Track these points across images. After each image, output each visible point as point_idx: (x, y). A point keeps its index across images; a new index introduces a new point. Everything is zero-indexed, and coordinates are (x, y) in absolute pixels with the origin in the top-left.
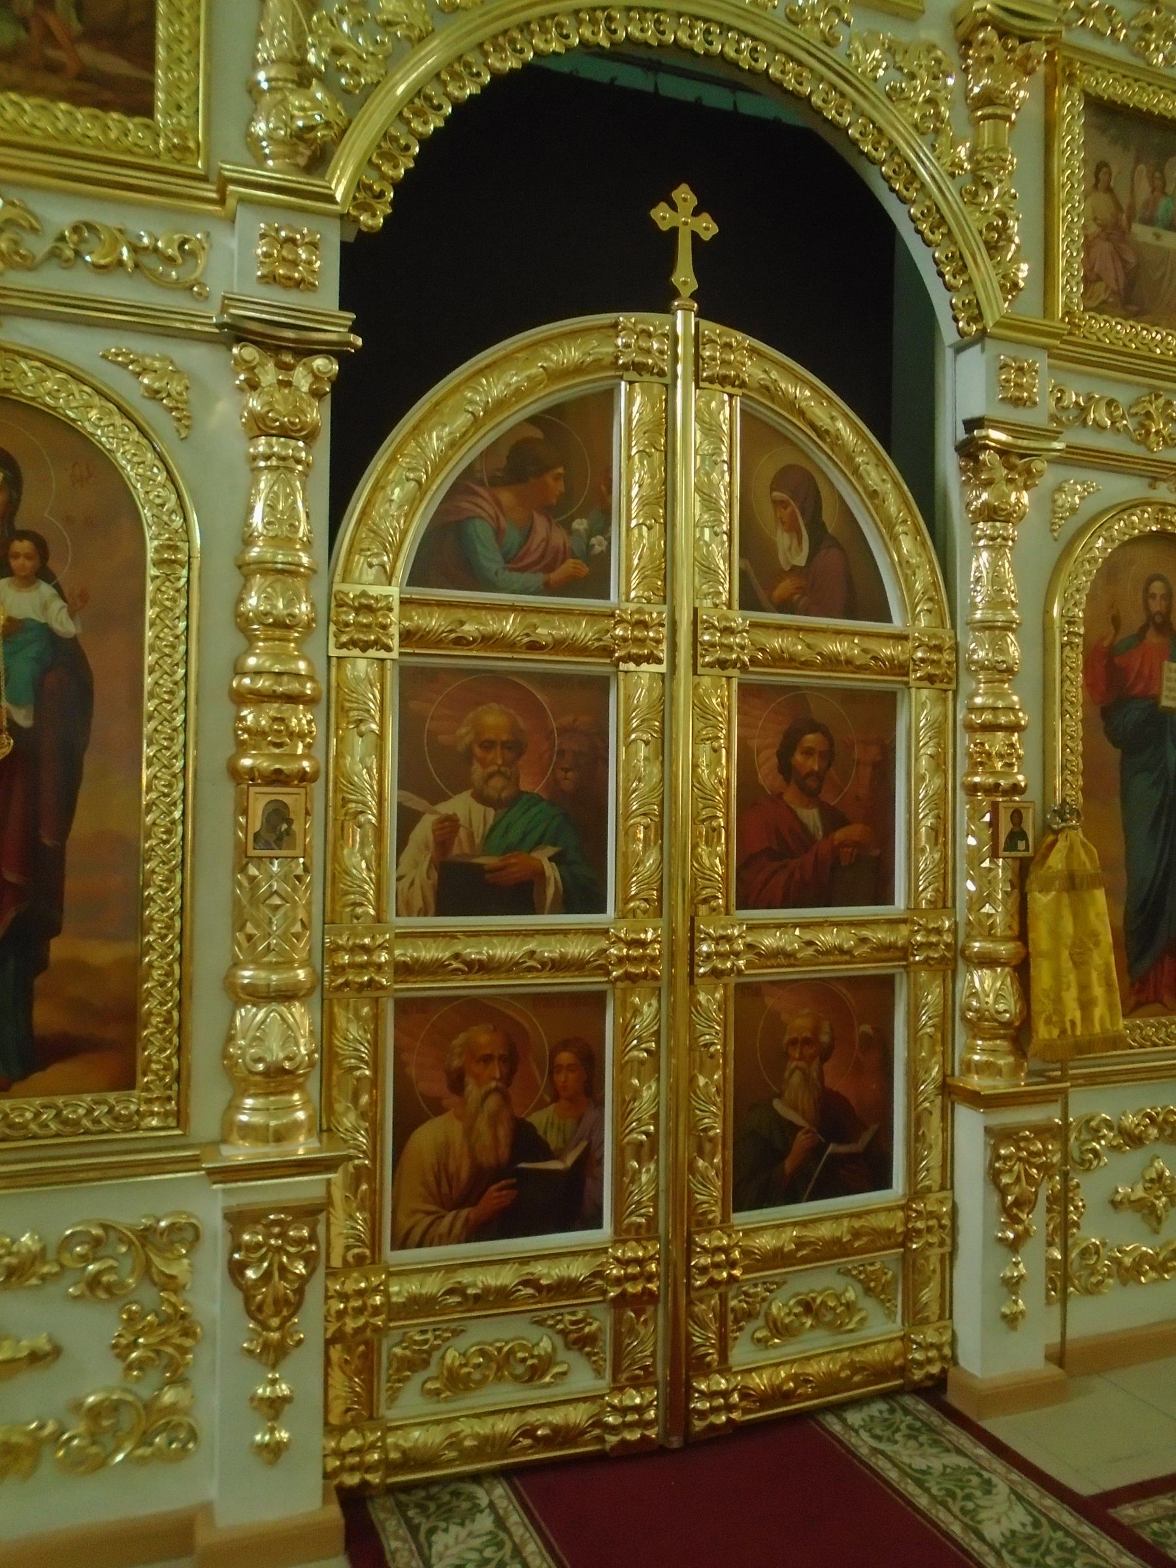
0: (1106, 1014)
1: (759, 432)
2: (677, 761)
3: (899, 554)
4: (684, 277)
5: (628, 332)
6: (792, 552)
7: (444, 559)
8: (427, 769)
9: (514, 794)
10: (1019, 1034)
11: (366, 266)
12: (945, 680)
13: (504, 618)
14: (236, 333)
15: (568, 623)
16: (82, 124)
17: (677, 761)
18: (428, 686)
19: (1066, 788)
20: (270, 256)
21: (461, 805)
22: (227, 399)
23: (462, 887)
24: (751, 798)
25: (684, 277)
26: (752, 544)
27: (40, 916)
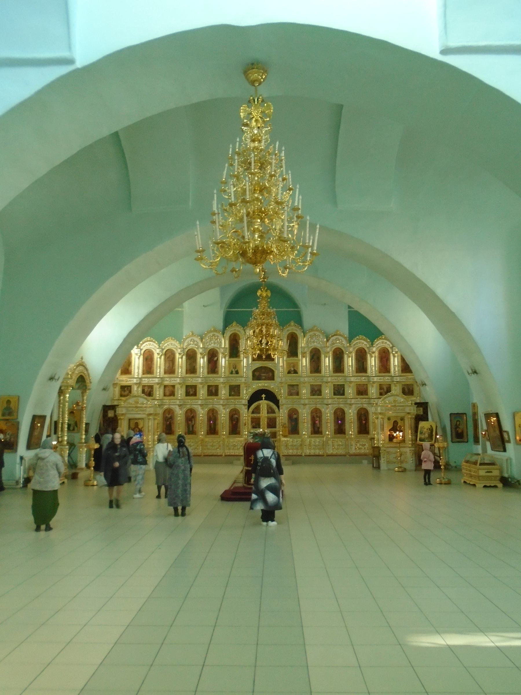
0: (287, 434)
1: (268, 405)
2: (264, 422)
3: (276, 410)
4: (264, 398)
5: (261, 402)
6: (270, 411)
7: (253, 413)
8: (252, 422)
9: (256, 423)
10: (282, 435)
11: (249, 401)
12: (279, 417)
13: (255, 415)
14: (243, 405)
15: (258, 415)
16: (238, 397)
17: (264, 422)
18: (252, 418)
19: (287, 422)
20: (245, 402)
21: (254, 424)
22: (243, 407)
23: (254, 427)
24: (268, 423)
25: (264, 398)
26: (268, 411)
27: (237, 429)
